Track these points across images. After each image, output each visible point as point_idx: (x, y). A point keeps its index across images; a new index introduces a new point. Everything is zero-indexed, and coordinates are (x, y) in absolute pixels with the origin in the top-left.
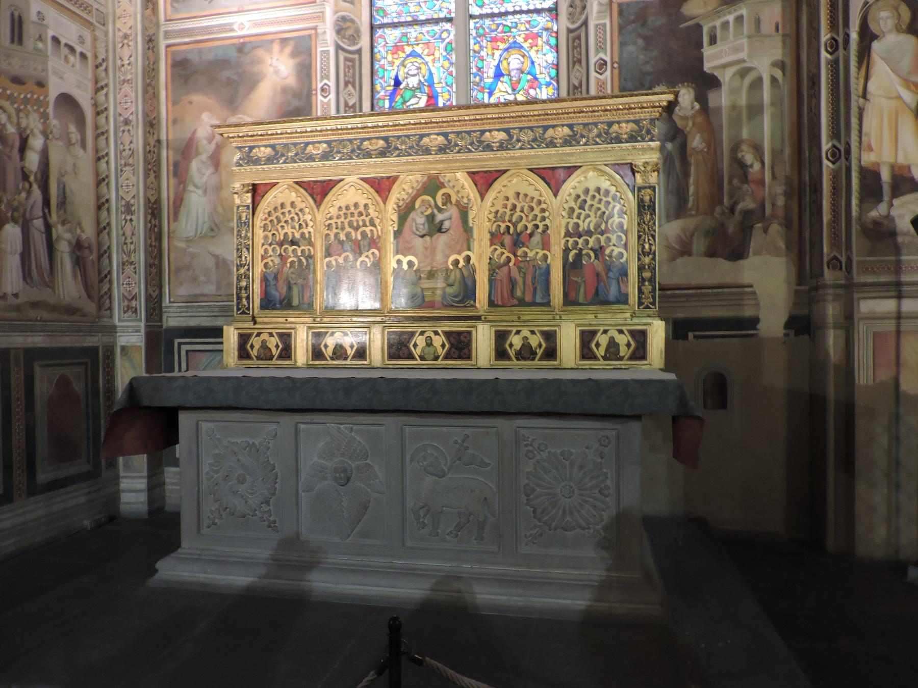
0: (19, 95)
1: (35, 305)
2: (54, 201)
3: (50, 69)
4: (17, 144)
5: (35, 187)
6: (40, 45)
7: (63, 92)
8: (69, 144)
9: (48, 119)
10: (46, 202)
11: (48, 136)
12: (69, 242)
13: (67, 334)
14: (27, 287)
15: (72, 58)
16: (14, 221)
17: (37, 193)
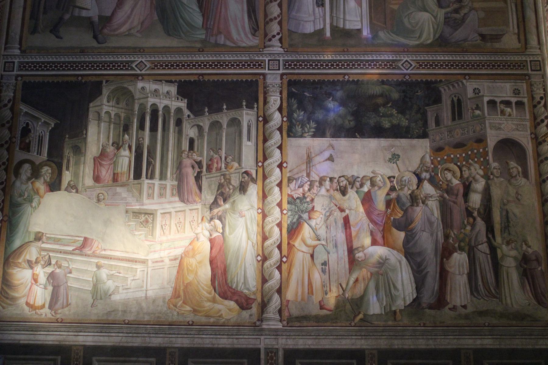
0: (461, 155)
1: (481, 313)
2: (497, 227)
3: (487, 125)
4: (461, 190)
5: (479, 219)
6: (477, 112)
7: (500, 138)
8: (511, 177)
9: (488, 164)
10: (490, 229)
11: (490, 177)
12: (515, 258)
13: (517, 337)
14: (474, 299)
15: (509, 110)
16: (461, 249)
17: (481, 224)
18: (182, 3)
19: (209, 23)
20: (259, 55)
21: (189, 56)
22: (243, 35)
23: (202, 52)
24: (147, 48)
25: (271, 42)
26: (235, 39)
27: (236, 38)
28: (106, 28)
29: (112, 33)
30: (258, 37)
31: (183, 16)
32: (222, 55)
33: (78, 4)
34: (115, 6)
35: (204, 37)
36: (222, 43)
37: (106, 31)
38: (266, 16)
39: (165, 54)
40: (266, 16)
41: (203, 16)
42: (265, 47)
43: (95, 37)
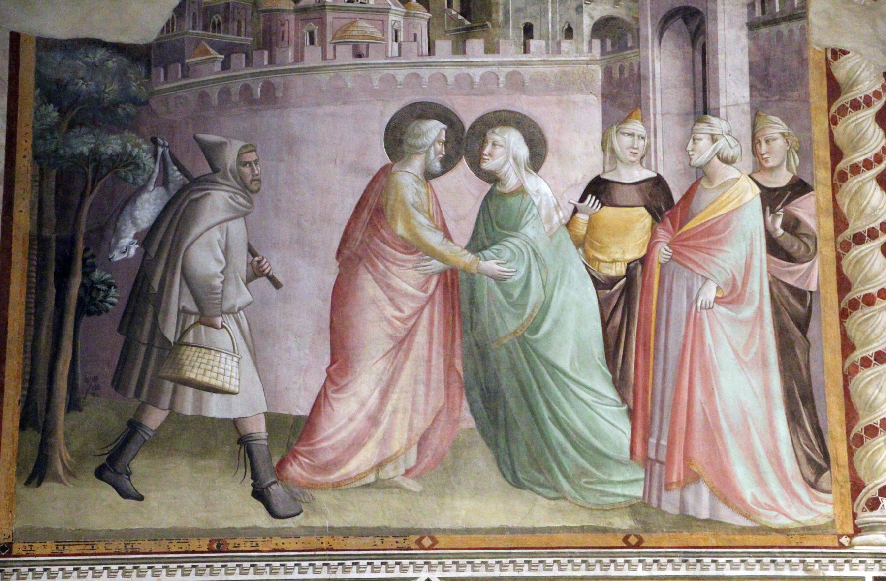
18: (555, 367)
19: (653, 441)
20: (839, 560)
21: (592, 561)
22: (775, 487)
23: (637, 546)
24: (444, 531)
25: (877, 512)
26: (748, 498)
27: (753, 496)
28: (295, 457)
29: (319, 478)
30: (829, 492)
31: (561, 414)
32: (707, 560)
33: (192, 374)
34: (323, 381)
35: (638, 491)
36: (705, 514)
37: (295, 470)
38: (851, 414)
39: (509, 556)
40: (851, 414)
41: (632, 414)
42: (857, 531)
43: (260, 494)
